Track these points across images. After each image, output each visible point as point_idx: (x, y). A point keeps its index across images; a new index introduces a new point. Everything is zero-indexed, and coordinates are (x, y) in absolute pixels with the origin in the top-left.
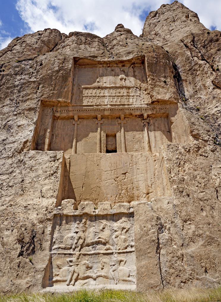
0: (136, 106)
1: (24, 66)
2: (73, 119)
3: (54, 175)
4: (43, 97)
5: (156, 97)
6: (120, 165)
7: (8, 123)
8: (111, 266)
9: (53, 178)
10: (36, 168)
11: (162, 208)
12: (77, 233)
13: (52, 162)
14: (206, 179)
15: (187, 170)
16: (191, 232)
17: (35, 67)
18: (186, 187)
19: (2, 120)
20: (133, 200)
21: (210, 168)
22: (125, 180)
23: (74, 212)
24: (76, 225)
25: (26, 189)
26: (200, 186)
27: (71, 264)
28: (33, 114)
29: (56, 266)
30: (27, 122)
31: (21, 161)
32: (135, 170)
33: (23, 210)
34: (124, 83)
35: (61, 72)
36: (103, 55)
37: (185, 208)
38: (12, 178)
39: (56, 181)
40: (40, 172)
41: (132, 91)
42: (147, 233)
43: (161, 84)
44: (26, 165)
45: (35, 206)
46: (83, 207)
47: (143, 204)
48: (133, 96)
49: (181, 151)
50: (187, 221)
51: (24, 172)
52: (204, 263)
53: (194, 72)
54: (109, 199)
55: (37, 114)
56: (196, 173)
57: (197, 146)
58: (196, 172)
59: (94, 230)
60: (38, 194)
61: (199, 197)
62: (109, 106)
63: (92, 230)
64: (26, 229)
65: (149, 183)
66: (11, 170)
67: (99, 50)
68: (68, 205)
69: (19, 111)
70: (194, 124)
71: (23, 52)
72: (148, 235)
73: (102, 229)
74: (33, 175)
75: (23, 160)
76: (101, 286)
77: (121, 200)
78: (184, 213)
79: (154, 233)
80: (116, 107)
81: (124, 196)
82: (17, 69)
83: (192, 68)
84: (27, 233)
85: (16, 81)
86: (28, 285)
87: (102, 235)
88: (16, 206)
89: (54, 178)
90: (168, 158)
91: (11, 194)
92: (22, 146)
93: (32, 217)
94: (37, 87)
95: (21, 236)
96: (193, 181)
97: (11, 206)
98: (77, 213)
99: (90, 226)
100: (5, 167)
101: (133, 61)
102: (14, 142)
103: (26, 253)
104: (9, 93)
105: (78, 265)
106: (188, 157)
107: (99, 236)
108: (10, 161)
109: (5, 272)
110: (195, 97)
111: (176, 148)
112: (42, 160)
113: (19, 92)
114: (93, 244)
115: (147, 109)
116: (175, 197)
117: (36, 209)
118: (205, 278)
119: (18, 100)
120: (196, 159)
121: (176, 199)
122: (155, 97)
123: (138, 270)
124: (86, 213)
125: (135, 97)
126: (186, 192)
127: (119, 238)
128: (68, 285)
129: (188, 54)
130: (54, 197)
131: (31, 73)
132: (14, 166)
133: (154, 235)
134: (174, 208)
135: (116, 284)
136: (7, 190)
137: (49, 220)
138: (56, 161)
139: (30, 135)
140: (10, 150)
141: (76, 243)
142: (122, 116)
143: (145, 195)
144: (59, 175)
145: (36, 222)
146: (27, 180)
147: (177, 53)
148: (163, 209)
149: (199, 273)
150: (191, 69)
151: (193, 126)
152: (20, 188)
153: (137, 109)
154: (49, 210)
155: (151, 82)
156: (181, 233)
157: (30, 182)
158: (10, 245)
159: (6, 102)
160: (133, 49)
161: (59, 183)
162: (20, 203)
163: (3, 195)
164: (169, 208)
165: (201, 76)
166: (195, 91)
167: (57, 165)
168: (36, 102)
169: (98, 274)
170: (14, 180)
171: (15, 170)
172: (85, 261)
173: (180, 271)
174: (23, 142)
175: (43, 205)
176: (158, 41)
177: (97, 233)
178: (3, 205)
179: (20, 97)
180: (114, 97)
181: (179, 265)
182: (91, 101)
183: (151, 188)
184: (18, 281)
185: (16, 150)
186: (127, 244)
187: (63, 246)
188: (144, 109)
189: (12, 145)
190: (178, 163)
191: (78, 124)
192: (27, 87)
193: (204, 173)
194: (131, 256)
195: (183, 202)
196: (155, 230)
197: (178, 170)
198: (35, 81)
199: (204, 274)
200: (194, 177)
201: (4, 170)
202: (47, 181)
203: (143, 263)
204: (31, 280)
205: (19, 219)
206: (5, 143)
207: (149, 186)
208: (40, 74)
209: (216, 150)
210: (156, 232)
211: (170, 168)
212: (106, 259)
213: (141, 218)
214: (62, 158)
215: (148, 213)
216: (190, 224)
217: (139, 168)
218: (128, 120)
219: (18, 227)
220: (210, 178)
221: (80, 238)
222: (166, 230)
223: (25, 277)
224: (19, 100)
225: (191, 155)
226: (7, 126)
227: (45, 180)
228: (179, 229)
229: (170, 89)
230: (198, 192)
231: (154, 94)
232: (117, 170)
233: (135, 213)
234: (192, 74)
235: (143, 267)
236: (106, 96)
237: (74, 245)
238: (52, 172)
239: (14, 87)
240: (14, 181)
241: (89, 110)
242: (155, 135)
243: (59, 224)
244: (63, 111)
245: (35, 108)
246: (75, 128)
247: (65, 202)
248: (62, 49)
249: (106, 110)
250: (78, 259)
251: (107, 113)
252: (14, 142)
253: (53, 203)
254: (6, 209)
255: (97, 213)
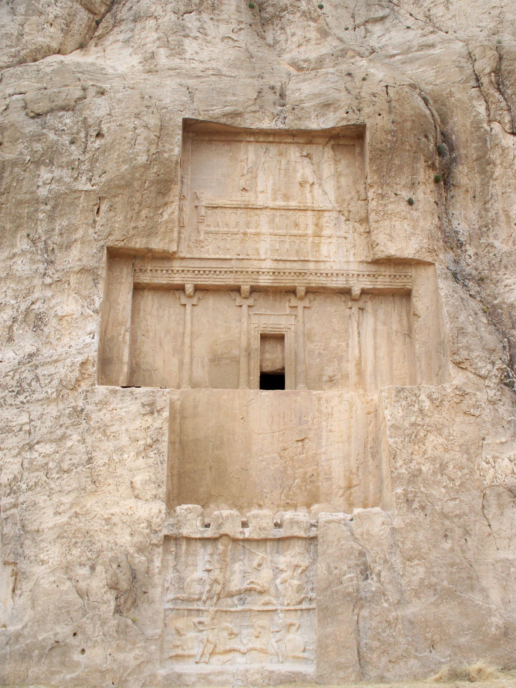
0: (334, 268)
1: (55, 138)
2: (181, 291)
3: (154, 447)
4: (111, 238)
5: (385, 250)
6: (291, 421)
7: (33, 307)
8: (273, 632)
9: (152, 454)
10: (113, 429)
11: (370, 533)
12: (209, 571)
13: (146, 418)
14: (466, 471)
15: (429, 451)
16: (416, 579)
17: (84, 140)
18: (422, 489)
19: (17, 294)
20: (317, 502)
21: (481, 444)
22: (302, 456)
23: (201, 532)
24: (207, 558)
25: (100, 478)
26: (451, 485)
27: (201, 628)
28: (89, 287)
29: (174, 632)
30: (79, 308)
31: (78, 412)
32: (324, 434)
33: (103, 526)
34: (308, 195)
35: (155, 170)
36: (257, 108)
37: (412, 535)
38: (65, 451)
39: (159, 463)
40: (124, 440)
41: (327, 222)
42: (339, 580)
43: (400, 208)
44: (91, 423)
45: (125, 518)
46: (220, 522)
47: (336, 522)
48: (330, 237)
49: (424, 404)
50: (413, 558)
51: (89, 439)
52: (430, 634)
53: (488, 168)
54: (266, 497)
55: (101, 285)
56: (447, 456)
57: (460, 393)
58: (448, 456)
59: (242, 569)
60: (124, 490)
61: (446, 510)
62: (268, 265)
63: (237, 567)
64: (119, 566)
65: (353, 465)
66: (59, 433)
67: (240, 29)
68: (189, 516)
69: (57, 276)
70: (464, 331)
71: (22, 35)
72: (342, 583)
73: (256, 566)
74: (109, 446)
75: (82, 410)
76: (256, 666)
77: (291, 500)
78: (409, 545)
79: (351, 579)
80: (288, 265)
81: (298, 491)
82: (38, 147)
83: (484, 156)
84: (122, 574)
85: (38, 187)
86: (139, 662)
87: (256, 578)
88: (87, 516)
89: (155, 454)
90: (393, 422)
91: (70, 488)
92: (77, 374)
93: (124, 541)
94: (96, 208)
95: (113, 578)
96: (439, 476)
97: (76, 517)
98: (209, 533)
99: (234, 560)
100: (45, 425)
101: (334, 132)
102: (56, 361)
103: (125, 609)
104: (24, 217)
105: (213, 629)
106: (437, 420)
107: (251, 580)
108: (53, 410)
109: (96, 641)
110: (482, 241)
111: (414, 398)
112: (124, 410)
113: (51, 218)
114: (239, 593)
115: (361, 276)
116: (396, 512)
117: (128, 523)
118: (427, 656)
119: (49, 242)
120: (453, 424)
121: (397, 516)
122: (382, 248)
123: (319, 641)
124: (226, 535)
125: (334, 240)
126: (419, 502)
127: (287, 585)
128: (197, 663)
129: (480, 111)
130: (160, 498)
131: (77, 163)
132: (64, 424)
133: (351, 584)
134: (393, 534)
135: (282, 662)
136: (58, 478)
137: (157, 545)
138: (156, 414)
139: (92, 345)
140: (50, 383)
141: (209, 591)
142: (301, 291)
143: (341, 492)
144: (164, 446)
145: (131, 551)
146: (100, 459)
147: (453, 99)
148: (371, 535)
149: (420, 648)
150: (481, 158)
151: (460, 338)
152: (87, 477)
153: (337, 274)
154: (153, 526)
155: (377, 206)
156: (399, 581)
157: (105, 463)
158: (97, 594)
159: (18, 244)
160: (337, 95)
161: (165, 465)
162: (95, 511)
163: (53, 491)
164: (382, 535)
165: (504, 183)
166: (484, 223)
167: (157, 425)
168: (95, 251)
169: (251, 646)
170: (70, 457)
171: (69, 432)
172: (228, 623)
173: (390, 644)
174: (78, 365)
175: (140, 514)
176: (411, 15)
177: (247, 574)
178: (60, 514)
179: (53, 233)
180: (283, 238)
181: (388, 635)
182: (228, 246)
183: (355, 476)
184: (120, 656)
185: (64, 384)
186: (303, 596)
187: (185, 596)
188: (353, 275)
189: (51, 369)
190: (413, 435)
191: (193, 305)
192: (72, 204)
193: (465, 456)
194: (309, 618)
195: (411, 523)
196: (352, 575)
197: (410, 451)
198: (91, 191)
199: (427, 650)
200: (441, 465)
201: (45, 430)
202: (141, 462)
203: (329, 629)
204: (141, 653)
205: (100, 544)
206: (34, 362)
207: (351, 472)
208: (100, 172)
209: (500, 400)
210: (355, 579)
211: (397, 447)
212: (263, 621)
213: (330, 551)
214: (168, 409)
215: (344, 542)
216: (417, 565)
217: (333, 428)
218: (315, 299)
219: (105, 562)
220: (476, 468)
221: (216, 581)
222: (374, 576)
223: (131, 650)
224: (54, 243)
225: (444, 414)
226: (32, 316)
227: (135, 460)
228: (396, 573)
229: (422, 223)
230: (445, 499)
231: (380, 237)
232: (284, 434)
233: (320, 540)
234: (483, 172)
235: (330, 636)
236: (264, 234)
237: (205, 594)
238: (149, 441)
239: (34, 202)
240: (70, 459)
241: (220, 272)
242: (375, 343)
243: (174, 553)
244: (159, 272)
245: (93, 269)
246: (188, 317)
247: (183, 511)
248: (132, 26)
249: (263, 273)
250: (213, 619)
251: (264, 281)
252: (56, 361)
253: (160, 512)
254: (68, 523)
255: (247, 536)
